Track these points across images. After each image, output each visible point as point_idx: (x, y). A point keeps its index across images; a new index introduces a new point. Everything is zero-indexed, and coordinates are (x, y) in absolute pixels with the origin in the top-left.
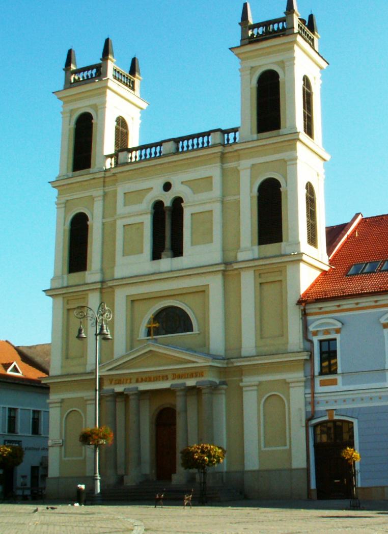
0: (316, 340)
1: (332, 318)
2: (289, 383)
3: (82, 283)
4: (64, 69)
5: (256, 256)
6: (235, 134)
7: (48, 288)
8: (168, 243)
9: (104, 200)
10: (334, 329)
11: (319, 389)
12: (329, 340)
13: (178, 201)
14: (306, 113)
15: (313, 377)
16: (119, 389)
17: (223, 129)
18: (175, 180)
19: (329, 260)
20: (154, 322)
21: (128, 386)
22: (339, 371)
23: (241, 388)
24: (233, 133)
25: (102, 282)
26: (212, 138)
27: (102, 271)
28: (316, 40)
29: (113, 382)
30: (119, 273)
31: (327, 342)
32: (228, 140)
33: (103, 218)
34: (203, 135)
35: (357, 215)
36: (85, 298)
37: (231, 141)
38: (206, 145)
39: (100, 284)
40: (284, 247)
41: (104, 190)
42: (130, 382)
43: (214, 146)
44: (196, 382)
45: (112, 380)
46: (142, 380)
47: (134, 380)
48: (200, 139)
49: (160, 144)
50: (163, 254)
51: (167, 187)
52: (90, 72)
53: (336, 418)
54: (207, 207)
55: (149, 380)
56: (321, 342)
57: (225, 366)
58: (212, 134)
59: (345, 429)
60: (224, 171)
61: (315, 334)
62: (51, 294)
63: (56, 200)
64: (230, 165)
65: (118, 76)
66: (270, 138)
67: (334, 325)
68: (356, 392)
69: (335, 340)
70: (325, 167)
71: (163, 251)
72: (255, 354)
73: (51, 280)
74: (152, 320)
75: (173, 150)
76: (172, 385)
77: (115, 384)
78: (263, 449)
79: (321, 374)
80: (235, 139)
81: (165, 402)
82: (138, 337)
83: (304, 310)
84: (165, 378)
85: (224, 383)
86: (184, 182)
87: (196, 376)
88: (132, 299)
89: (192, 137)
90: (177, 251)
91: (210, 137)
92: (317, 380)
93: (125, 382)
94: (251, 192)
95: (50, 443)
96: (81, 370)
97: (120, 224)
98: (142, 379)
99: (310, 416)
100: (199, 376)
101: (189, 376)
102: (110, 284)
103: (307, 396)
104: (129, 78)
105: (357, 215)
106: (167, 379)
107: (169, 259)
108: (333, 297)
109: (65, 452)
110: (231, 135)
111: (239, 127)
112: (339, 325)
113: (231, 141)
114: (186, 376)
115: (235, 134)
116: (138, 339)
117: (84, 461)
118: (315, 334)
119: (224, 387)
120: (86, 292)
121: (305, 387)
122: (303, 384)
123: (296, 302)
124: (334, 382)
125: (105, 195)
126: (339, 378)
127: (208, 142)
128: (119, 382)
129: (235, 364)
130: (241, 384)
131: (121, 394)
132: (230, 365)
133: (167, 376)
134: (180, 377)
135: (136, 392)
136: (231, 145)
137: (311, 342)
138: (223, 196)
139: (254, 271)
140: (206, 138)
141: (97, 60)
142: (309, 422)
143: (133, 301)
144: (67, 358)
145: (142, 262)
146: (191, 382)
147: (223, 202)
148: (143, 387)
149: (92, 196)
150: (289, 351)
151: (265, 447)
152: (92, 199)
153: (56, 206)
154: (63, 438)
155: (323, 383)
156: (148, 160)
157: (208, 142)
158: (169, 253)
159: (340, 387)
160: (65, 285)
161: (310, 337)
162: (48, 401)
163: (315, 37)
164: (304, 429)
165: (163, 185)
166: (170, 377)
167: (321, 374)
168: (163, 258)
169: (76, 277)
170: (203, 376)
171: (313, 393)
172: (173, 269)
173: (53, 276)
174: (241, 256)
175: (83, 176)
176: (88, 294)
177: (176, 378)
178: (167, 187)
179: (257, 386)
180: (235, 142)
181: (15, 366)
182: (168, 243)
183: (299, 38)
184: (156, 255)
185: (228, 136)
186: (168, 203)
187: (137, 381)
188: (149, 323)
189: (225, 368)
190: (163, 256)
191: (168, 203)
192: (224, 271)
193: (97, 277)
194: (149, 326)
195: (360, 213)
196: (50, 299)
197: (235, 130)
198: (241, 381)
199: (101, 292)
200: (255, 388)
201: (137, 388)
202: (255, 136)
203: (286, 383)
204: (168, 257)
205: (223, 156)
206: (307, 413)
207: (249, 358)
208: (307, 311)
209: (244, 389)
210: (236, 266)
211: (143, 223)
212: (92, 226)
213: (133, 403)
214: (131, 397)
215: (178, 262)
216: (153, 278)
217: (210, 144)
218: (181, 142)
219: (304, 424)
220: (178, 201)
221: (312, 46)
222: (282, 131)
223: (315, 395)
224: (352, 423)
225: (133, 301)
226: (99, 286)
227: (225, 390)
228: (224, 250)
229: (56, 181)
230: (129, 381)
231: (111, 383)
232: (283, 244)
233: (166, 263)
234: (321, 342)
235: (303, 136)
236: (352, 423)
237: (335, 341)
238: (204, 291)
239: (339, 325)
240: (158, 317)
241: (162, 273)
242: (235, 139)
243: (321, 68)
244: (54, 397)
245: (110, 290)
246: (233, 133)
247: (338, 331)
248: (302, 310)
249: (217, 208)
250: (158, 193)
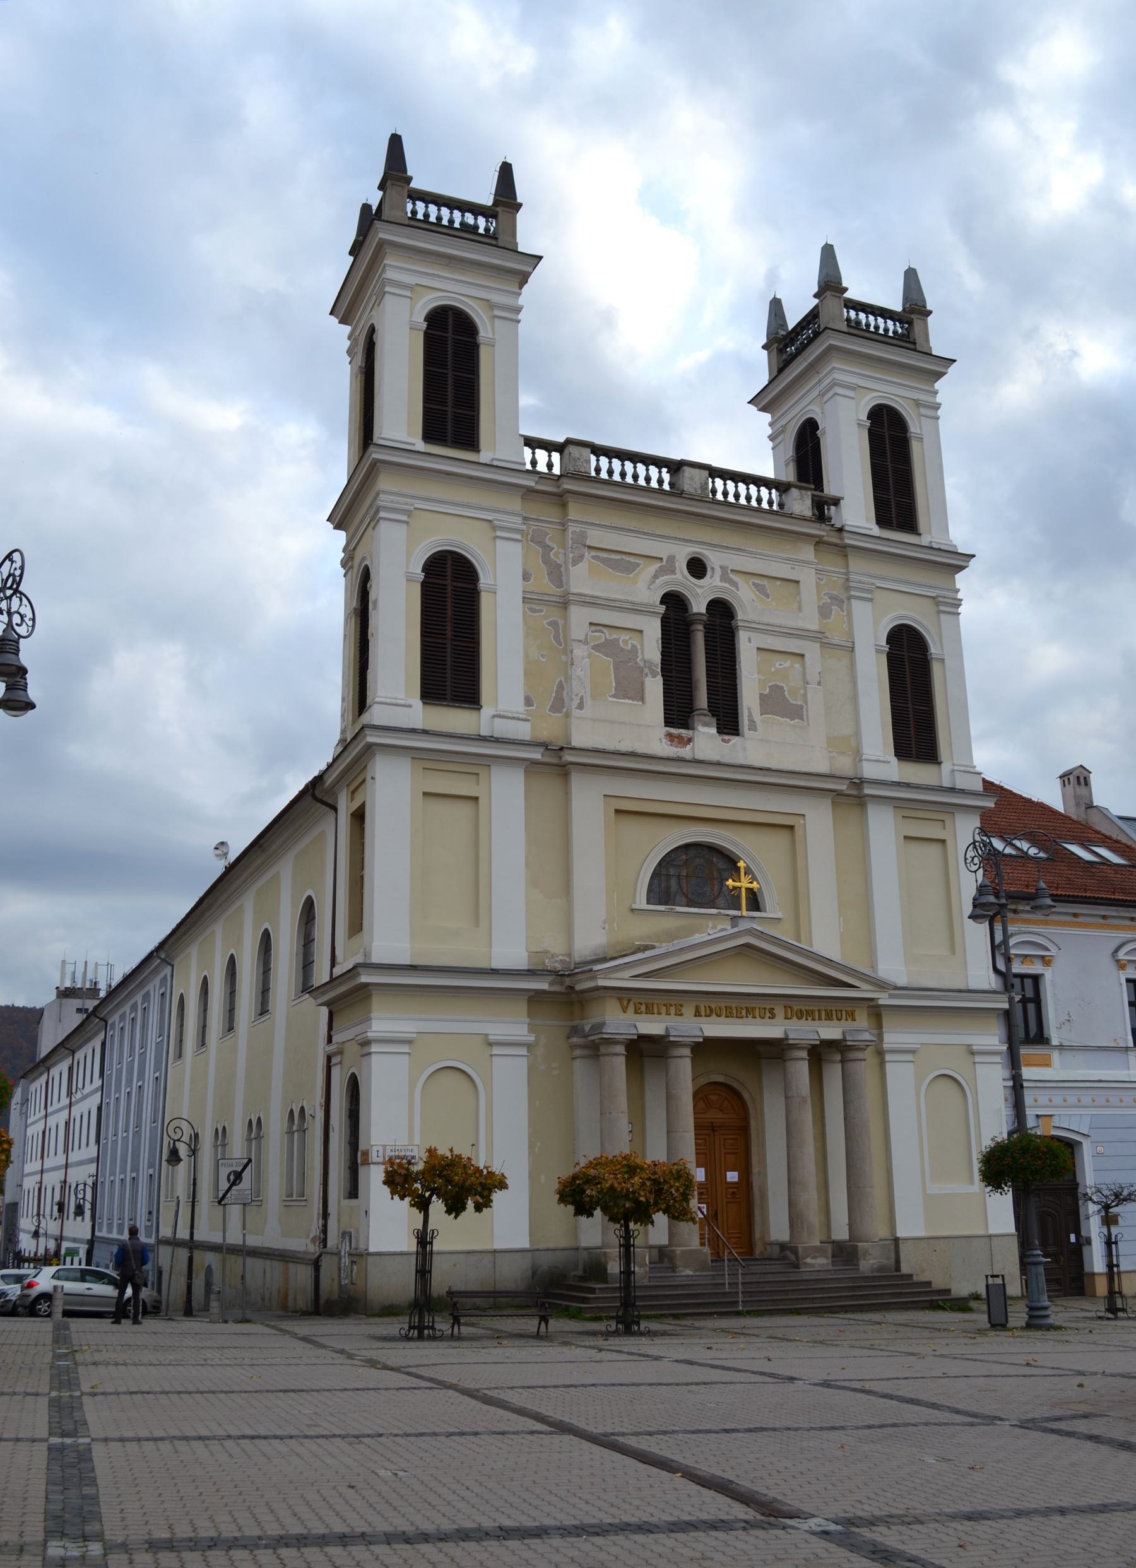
2: (973, 1053)
8: (702, 699)
10: (1043, 957)
44: (840, 1030)
46: (710, 1012)
51: (697, 567)
54: (793, 645)
84: (768, 1014)
101: (823, 1017)
106: (773, 1017)
114: (817, 1018)
116: (634, 906)
126: (1055, 1056)
170: (854, 1020)
178: (697, 567)
182: (702, 699)
186: (699, 606)
191: (699, 606)
209: (888, 1057)
220: (722, 611)
230: (673, 1010)
247: (1046, 961)
250: (681, 579)
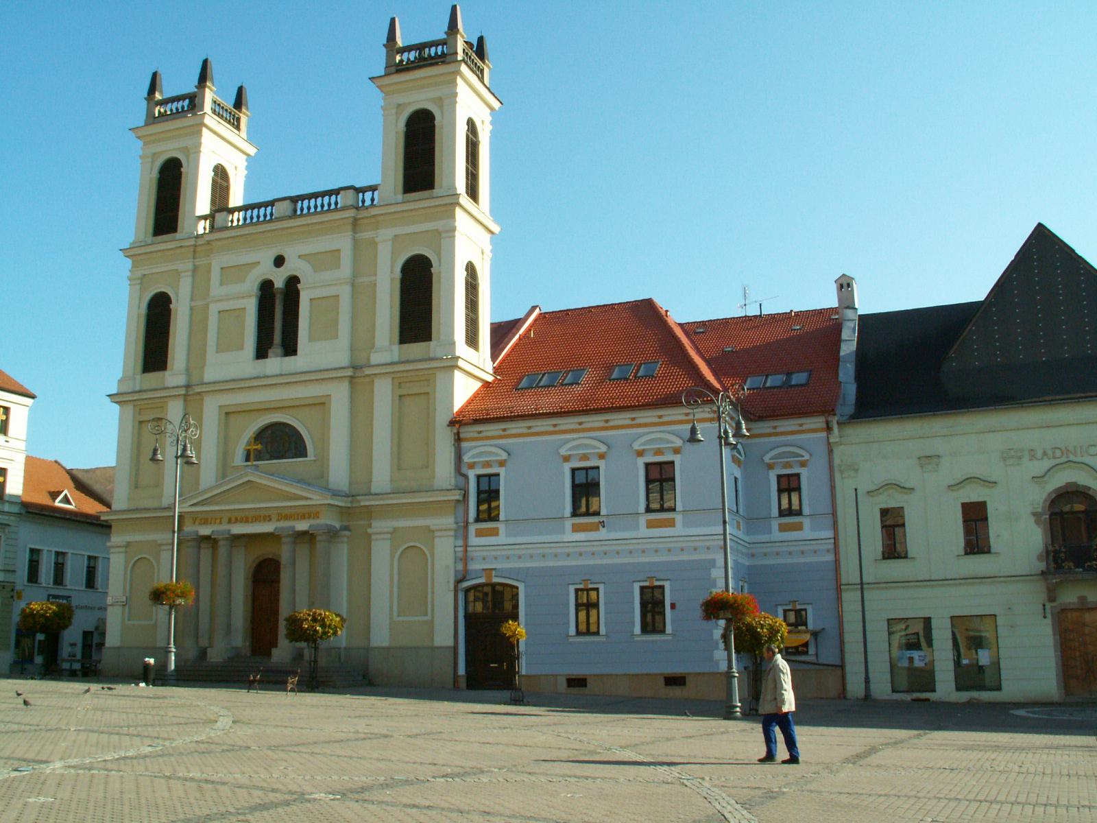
0: (472, 474)
1: (495, 446)
2: (433, 531)
3: (160, 386)
4: (145, 99)
5: (396, 359)
6: (373, 194)
7: (114, 391)
9: (193, 276)
10: (497, 461)
11: (474, 540)
12: (489, 476)
13: (293, 282)
14: (470, 168)
15: (467, 524)
16: (205, 531)
17: (357, 186)
18: (291, 253)
19: (494, 368)
20: (255, 442)
21: (216, 528)
22: (502, 517)
23: (369, 536)
24: (371, 192)
25: (188, 387)
26: (342, 199)
27: (188, 371)
28: (486, 71)
29: (197, 522)
30: (209, 375)
31: (584, 471)
32: (363, 201)
33: (192, 300)
34: (330, 193)
35: (534, 308)
36: (163, 407)
37: (368, 203)
38: (333, 207)
39: (184, 389)
40: (433, 347)
41: (193, 262)
42: (221, 523)
43: (344, 208)
44: (309, 525)
45: (196, 518)
46: (236, 521)
47: (225, 520)
48: (326, 199)
49: (271, 203)
50: (270, 352)
51: (279, 261)
52: (181, 103)
53: (495, 580)
55: (245, 520)
56: (479, 477)
57: (349, 505)
58: (342, 192)
59: (507, 596)
60: (356, 243)
61: (472, 466)
62: (119, 400)
63: (129, 274)
64: (365, 235)
65: (218, 110)
66: (420, 200)
67: (497, 455)
68: (523, 546)
69: (498, 475)
70: (492, 242)
71: (270, 348)
72: (389, 491)
73: (119, 381)
74: (253, 440)
75: (289, 212)
76: (276, 529)
77: (200, 524)
78: (396, 618)
79: (478, 520)
80: (373, 200)
81: (267, 551)
82: (233, 462)
83: (458, 433)
85: (347, 528)
86: (302, 255)
87: (309, 517)
88: (227, 411)
89: (315, 195)
90: (290, 348)
91: (339, 197)
92: (472, 529)
93: (213, 522)
94: (392, 272)
95: (109, 600)
96: (156, 505)
97: (214, 309)
98: (236, 519)
99: (460, 577)
100: (314, 518)
101: (300, 517)
102: (198, 389)
103: (457, 549)
104: (233, 113)
105: (534, 308)
106: (270, 520)
107: (279, 359)
108: (497, 417)
109: (130, 613)
110: (368, 195)
111: (379, 185)
112: (504, 456)
113: (368, 203)
115: (373, 194)
116: (233, 465)
117: (155, 626)
118: (472, 466)
119: (347, 533)
120: (166, 400)
121: (456, 537)
122: (452, 533)
123: (448, 423)
124: (495, 532)
125: (195, 269)
126: (502, 527)
127: (336, 203)
128: (205, 522)
129: (362, 504)
130: (369, 531)
131: (207, 538)
132: (355, 505)
133: (269, 516)
134: (288, 517)
135: (227, 536)
136: (367, 208)
137: (466, 477)
138: (355, 275)
139: (393, 378)
140: (333, 198)
141: (190, 87)
142: (459, 585)
143: (227, 414)
144: (136, 487)
145: (243, 361)
146: (302, 526)
147: (353, 285)
148: (238, 529)
149: (177, 270)
150: (435, 488)
151: (398, 616)
152: (177, 273)
153: (129, 282)
154: (128, 594)
155: (480, 533)
156: (255, 224)
157: (336, 203)
158: (279, 350)
159: (502, 539)
160: (137, 388)
161: (464, 470)
162: (109, 544)
163: (485, 67)
164: (452, 594)
165: (273, 259)
166: (274, 517)
167: (478, 520)
168: (271, 357)
169: (153, 378)
170: (318, 517)
171: (466, 546)
172: (283, 373)
173: (121, 375)
174: (376, 358)
175: (166, 243)
176: (167, 402)
177: (281, 519)
178: (279, 261)
179: (391, 533)
180: (372, 204)
181: (66, 495)
183: (464, 68)
184: (261, 353)
185: (363, 196)
186: (279, 283)
187: (230, 521)
188: (249, 443)
189: (349, 508)
190: (270, 354)
191: (279, 283)
192: (352, 377)
193: (181, 380)
194: (249, 448)
195: (537, 306)
196: (116, 407)
197: (373, 189)
198: (370, 526)
199: (185, 400)
200: (388, 536)
201: (229, 531)
202: (400, 197)
203: (430, 531)
204: (277, 356)
205: (355, 223)
206: (456, 571)
207: (381, 496)
208: (462, 436)
209: (373, 537)
210: (368, 371)
211: (245, 308)
212: (176, 310)
213: (223, 550)
214: (221, 543)
215: (291, 363)
216: (256, 383)
217: (339, 206)
218: (300, 202)
219: (452, 587)
220: (293, 282)
221: (481, 79)
222: (436, 192)
223: (468, 549)
224: (517, 588)
225: (228, 414)
226: (183, 392)
227: (348, 537)
228: (352, 349)
229: (130, 248)
230: (218, 521)
231: (194, 523)
232: (433, 344)
233: (275, 364)
234: (479, 477)
235: (465, 200)
236: (517, 588)
237: (497, 477)
238: (324, 404)
239: (504, 456)
240: (260, 436)
241: (268, 377)
242: (373, 200)
243: (492, 109)
244: (117, 539)
245: (198, 397)
246: (371, 192)
247: (502, 463)
248: (454, 433)
249: (345, 292)
250: (266, 270)
